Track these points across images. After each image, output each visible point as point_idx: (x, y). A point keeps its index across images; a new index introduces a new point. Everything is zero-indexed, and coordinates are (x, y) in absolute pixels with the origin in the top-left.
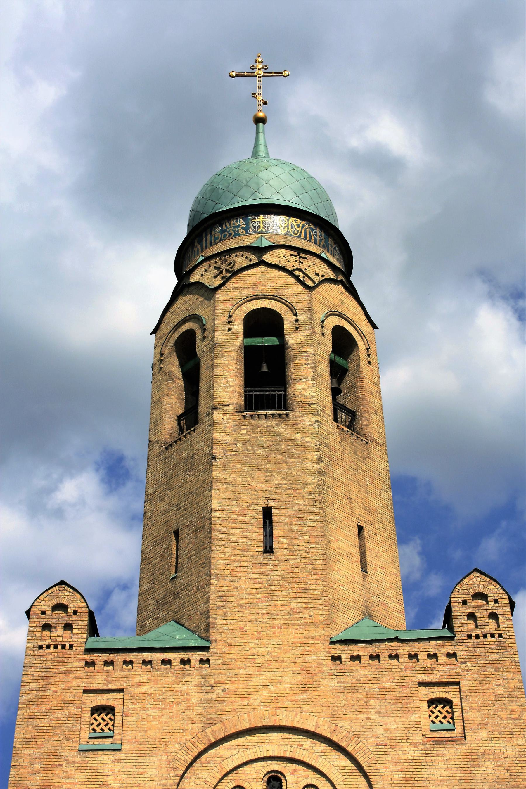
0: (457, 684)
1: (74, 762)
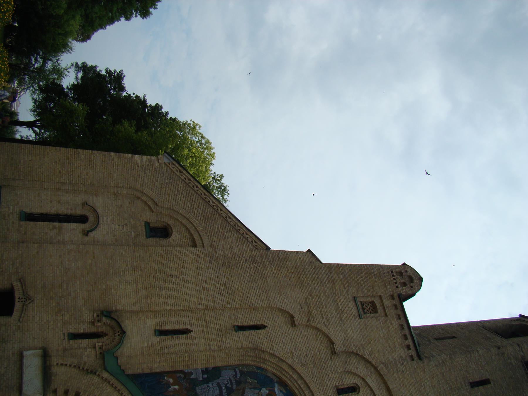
1: (348, 295)
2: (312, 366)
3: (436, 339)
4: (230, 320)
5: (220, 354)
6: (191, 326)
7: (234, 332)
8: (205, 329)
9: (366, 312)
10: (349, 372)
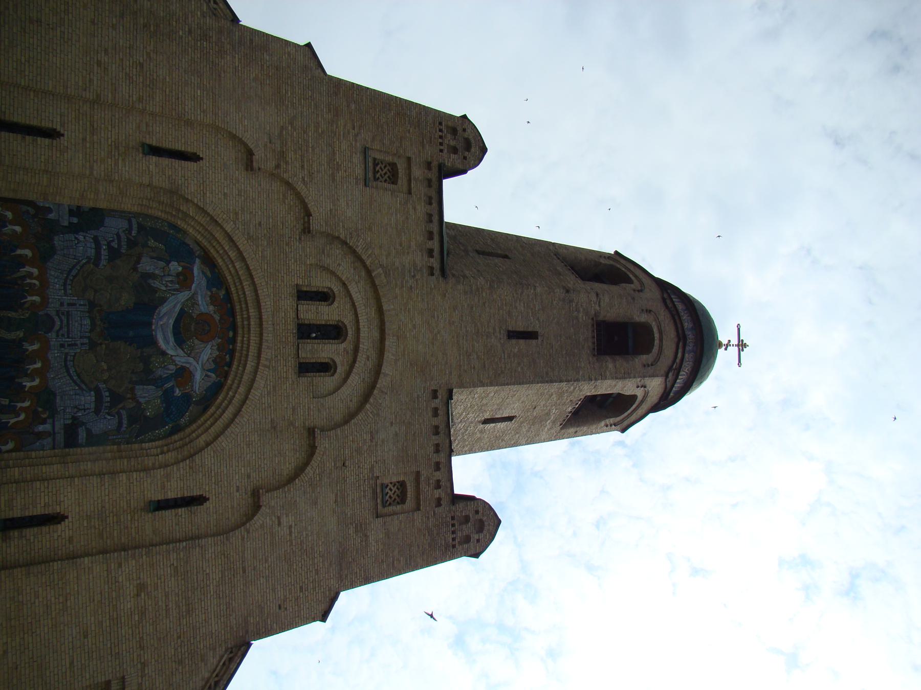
0: (418, 509)
1: (356, 141)
2: (265, 243)
3: (478, 252)
4: (138, 132)
5: (108, 188)
6: (63, 125)
7: (141, 155)
8: (88, 137)
9: (378, 178)
10: (325, 269)
